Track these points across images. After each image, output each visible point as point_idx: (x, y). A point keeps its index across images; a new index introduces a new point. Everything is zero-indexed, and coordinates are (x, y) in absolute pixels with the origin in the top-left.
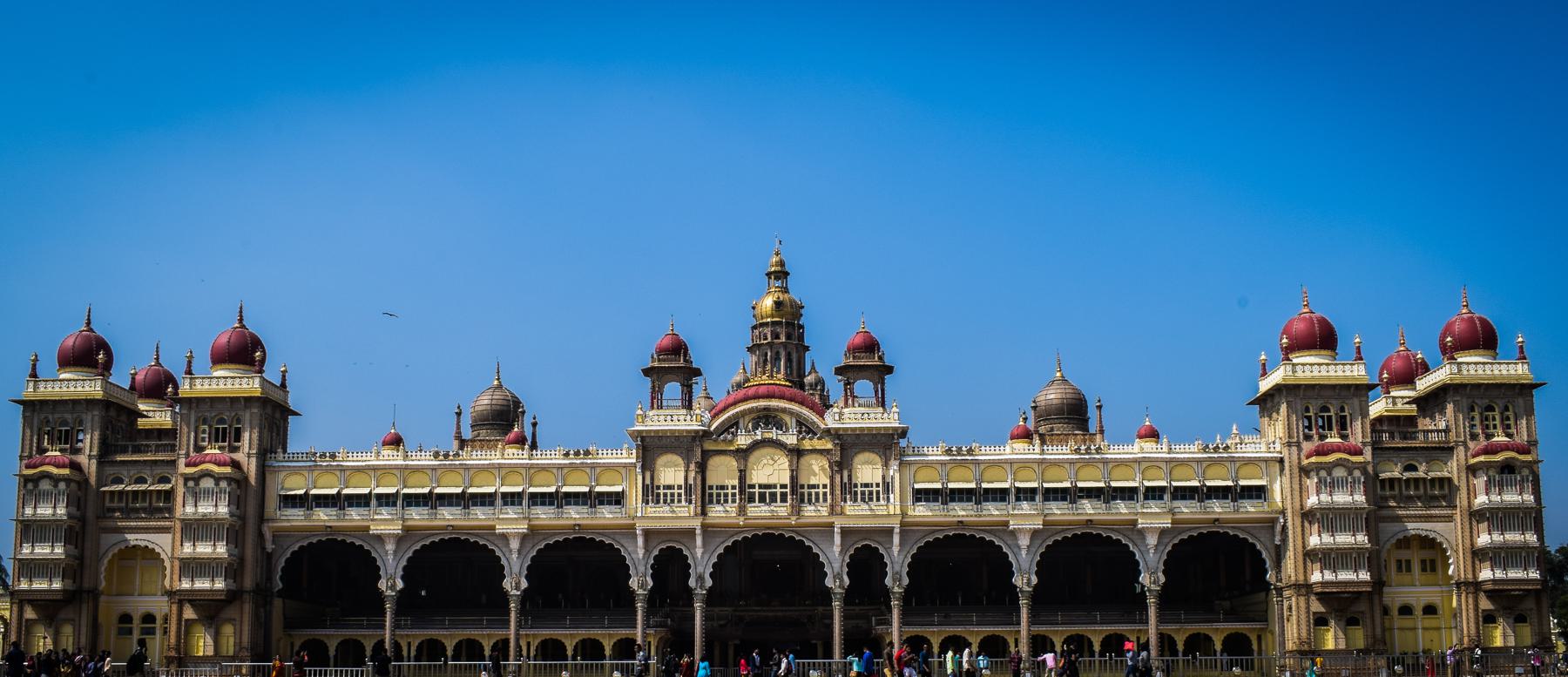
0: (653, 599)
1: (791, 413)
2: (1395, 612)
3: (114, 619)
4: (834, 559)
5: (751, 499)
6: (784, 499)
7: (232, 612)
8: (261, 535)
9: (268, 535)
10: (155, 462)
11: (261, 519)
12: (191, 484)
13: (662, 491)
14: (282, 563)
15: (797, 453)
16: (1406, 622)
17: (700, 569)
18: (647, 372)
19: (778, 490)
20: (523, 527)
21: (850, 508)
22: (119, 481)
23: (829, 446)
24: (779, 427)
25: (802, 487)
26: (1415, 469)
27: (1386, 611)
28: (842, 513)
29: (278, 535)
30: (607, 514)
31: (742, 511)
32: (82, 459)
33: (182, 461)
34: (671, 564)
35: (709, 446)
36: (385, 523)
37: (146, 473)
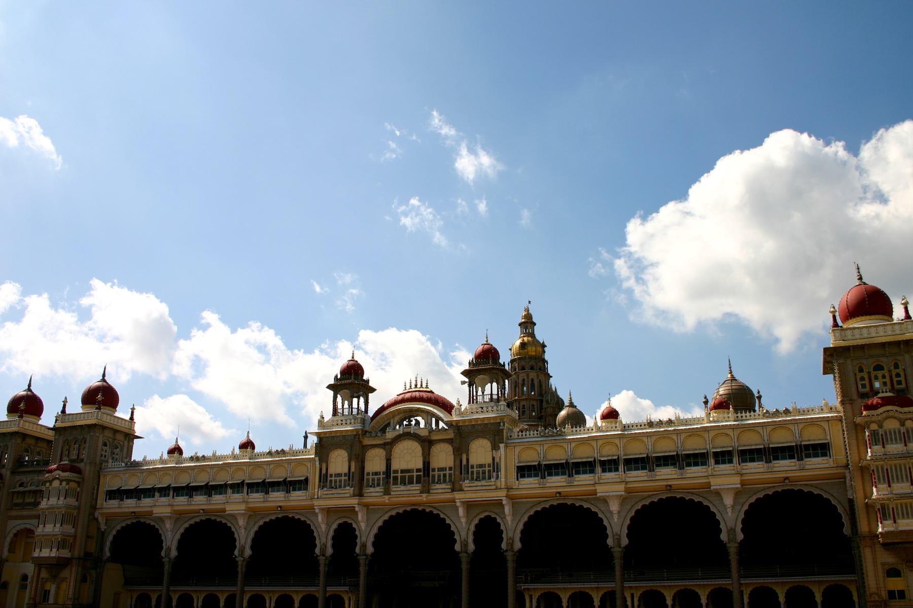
4: (463, 528)
5: (395, 483)
7: (65, 573)
9: (100, 519)
11: (94, 507)
13: (333, 478)
14: (111, 538)
17: (364, 539)
18: (330, 387)
19: (415, 474)
25: (434, 470)
30: (297, 497)
31: (387, 492)
34: (345, 534)
35: (367, 441)
36: (160, 507)
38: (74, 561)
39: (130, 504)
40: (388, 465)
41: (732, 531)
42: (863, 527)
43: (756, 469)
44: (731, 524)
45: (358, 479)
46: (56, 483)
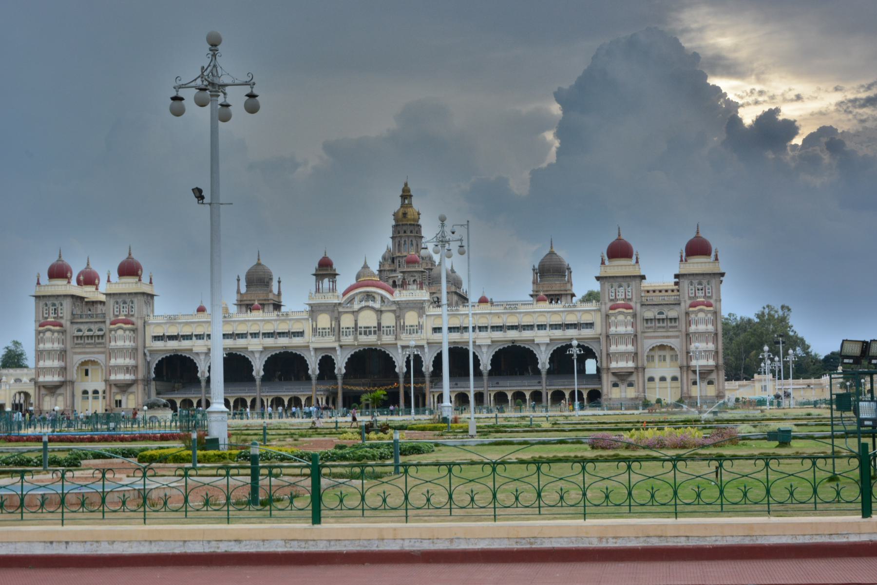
0: (320, 378)
1: (378, 294)
2: (657, 380)
3: (81, 393)
5: (361, 334)
6: (375, 332)
8: (145, 354)
9: (148, 354)
10: (96, 322)
11: (145, 347)
12: (113, 332)
15: (380, 312)
16: (663, 384)
19: (373, 329)
20: (260, 348)
21: (403, 336)
22: (79, 330)
23: (394, 308)
24: (374, 299)
26: (663, 313)
27: (651, 379)
28: (400, 339)
29: (152, 352)
30: (297, 341)
31: (356, 339)
32: (63, 321)
33: (108, 322)
34: (327, 363)
35: (341, 309)
37: (92, 327)
38: (140, 382)
39: (173, 345)
40: (356, 324)
41: (544, 363)
42: (604, 365)
43: (558, 333)
44: (543, 360)
45: (337, 331)
46: (120, 332)
